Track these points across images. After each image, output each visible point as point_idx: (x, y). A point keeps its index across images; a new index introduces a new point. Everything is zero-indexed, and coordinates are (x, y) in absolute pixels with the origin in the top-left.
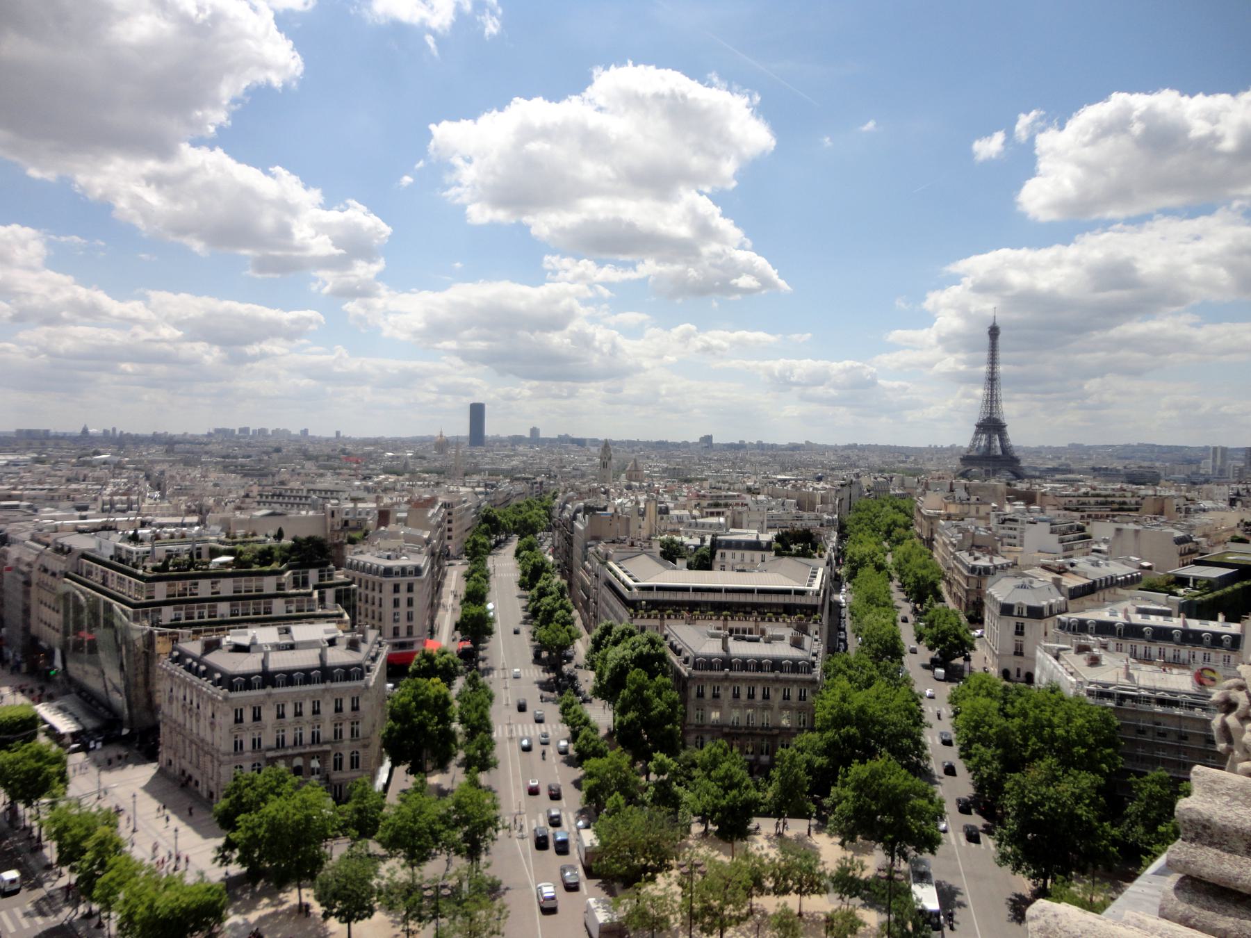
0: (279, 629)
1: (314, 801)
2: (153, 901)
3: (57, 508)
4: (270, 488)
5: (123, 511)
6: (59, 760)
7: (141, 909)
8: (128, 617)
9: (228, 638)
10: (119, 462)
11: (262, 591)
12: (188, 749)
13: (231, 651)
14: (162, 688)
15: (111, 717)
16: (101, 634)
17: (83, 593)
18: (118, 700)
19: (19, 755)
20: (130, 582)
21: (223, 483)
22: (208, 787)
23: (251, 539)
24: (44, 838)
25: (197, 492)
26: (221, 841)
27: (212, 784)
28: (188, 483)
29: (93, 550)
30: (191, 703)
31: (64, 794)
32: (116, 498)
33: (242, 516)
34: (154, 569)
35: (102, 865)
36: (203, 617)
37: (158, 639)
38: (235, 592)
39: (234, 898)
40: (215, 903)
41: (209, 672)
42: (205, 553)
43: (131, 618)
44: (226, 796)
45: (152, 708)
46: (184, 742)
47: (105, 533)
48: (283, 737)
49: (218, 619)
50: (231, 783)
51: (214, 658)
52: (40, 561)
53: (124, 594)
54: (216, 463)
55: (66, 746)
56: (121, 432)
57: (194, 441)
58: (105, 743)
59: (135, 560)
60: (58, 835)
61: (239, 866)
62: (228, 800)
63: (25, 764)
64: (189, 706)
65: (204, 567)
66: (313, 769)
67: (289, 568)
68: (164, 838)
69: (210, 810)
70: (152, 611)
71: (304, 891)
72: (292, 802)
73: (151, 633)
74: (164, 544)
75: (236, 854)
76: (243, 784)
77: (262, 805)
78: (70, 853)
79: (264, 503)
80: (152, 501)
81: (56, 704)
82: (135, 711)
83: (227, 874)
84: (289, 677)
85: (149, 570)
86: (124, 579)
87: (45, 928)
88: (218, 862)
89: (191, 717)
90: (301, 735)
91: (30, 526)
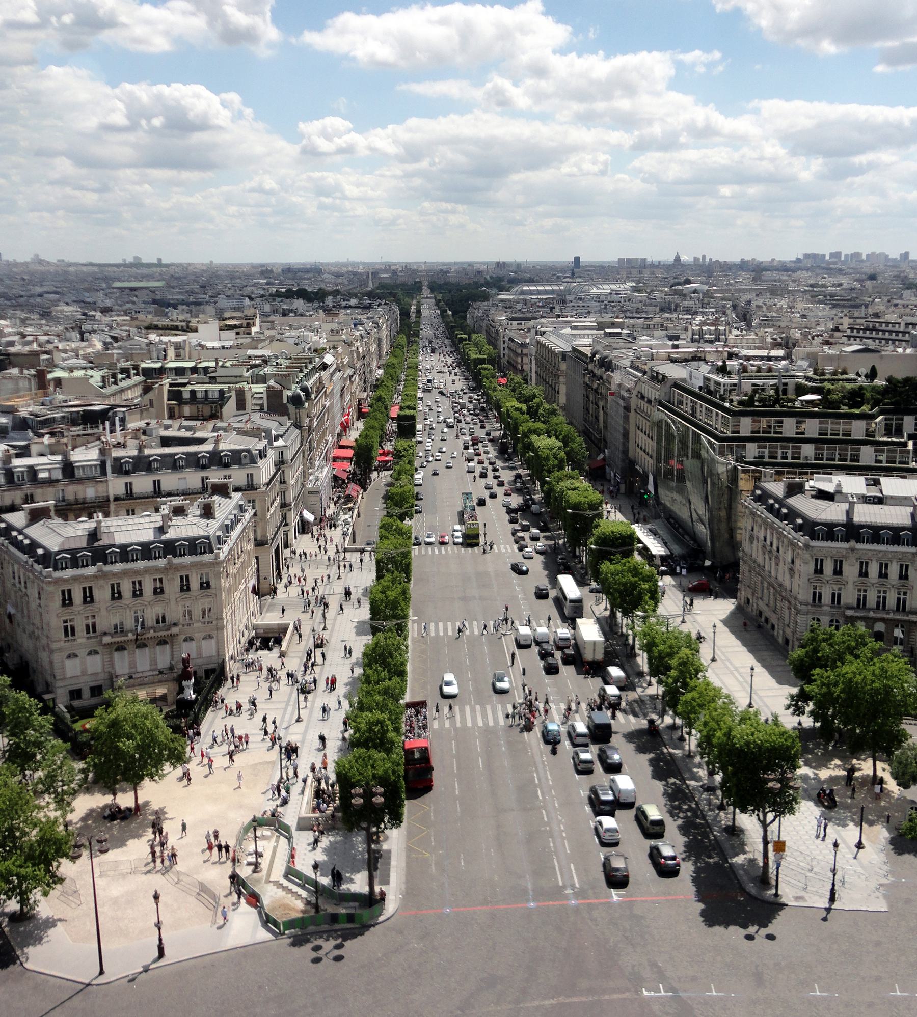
0: (866, 479)
1: (895, 673)
2: (730, 729)
3: (652, 336)
4: (863, 321)
5: (711, 342)
6: (650, 578)
7: (719, 734)
8: (714, 450)
9: (811, 483)
10: (708, 291)
11: (850, 435)
12: (765, 591)
13: (813, 497)
14: (744, 524)
15: (695, 547)
16: (690, 464)
17: (673, 421)
18: (702, 530)
19: (619, 567)
20: (717, 414)
21: (811, 314)
22: (784, 632)
23: (840, 377)
24: (637, 646)
25: (783, 324)
26: (795, 690)
27: (788, 631)
28: (774, 314)
29: (684, 380)
30: (771, 544)
31: (654, 611)
32: (705, 328)
33: (831, 352)
34: (741, 403)
35: (685, 685)
36: (786, 458)
37: (741, 475)
38: (820, 434)
39: (806, 750)
40: (788, 748)
41: (791, 515)
42: (791, 389)
43: (717, 450)
44: (802, 646)
45: (734, 545)
46: (762, 583)
47: (696, 363)
48: (865, 597)
49: (801, 461)
50: (807, 635)
51: (796, 502)
52: (637, 389)
53: (711, 426)
54: (806, 291)
55: (657, 567)
56: (711, 259)
57: (784, 268)
58: (689, 571)
59: (722, 393)
60: (649, 648)
61: (811, 719)
62: (804, 650)
63: (624, 577)
64: (768, 548)
65: (789, 404)
66: (896, 638)
67: (881, 412)
68: (740, 674)
69: (786, 657)
70: (737, 446)
71: (879, 765)
72: (871, 668)
73: (735, 468)
74: (750, 378)
75: (810, 707)
76: (821, 637)
77: (839, 664)
78: (658, 667)
79: (855, 337)
80: (738, 332)
81: (648, 526)
82: (717, 544)
83: (800, 724)
84: (876, 533)
85: (735, 403)
86: (712, 412)
87: (638, 727)
88: (791, 710)
89: (770, 559)
90: (885, 598)
91: (630, 353)
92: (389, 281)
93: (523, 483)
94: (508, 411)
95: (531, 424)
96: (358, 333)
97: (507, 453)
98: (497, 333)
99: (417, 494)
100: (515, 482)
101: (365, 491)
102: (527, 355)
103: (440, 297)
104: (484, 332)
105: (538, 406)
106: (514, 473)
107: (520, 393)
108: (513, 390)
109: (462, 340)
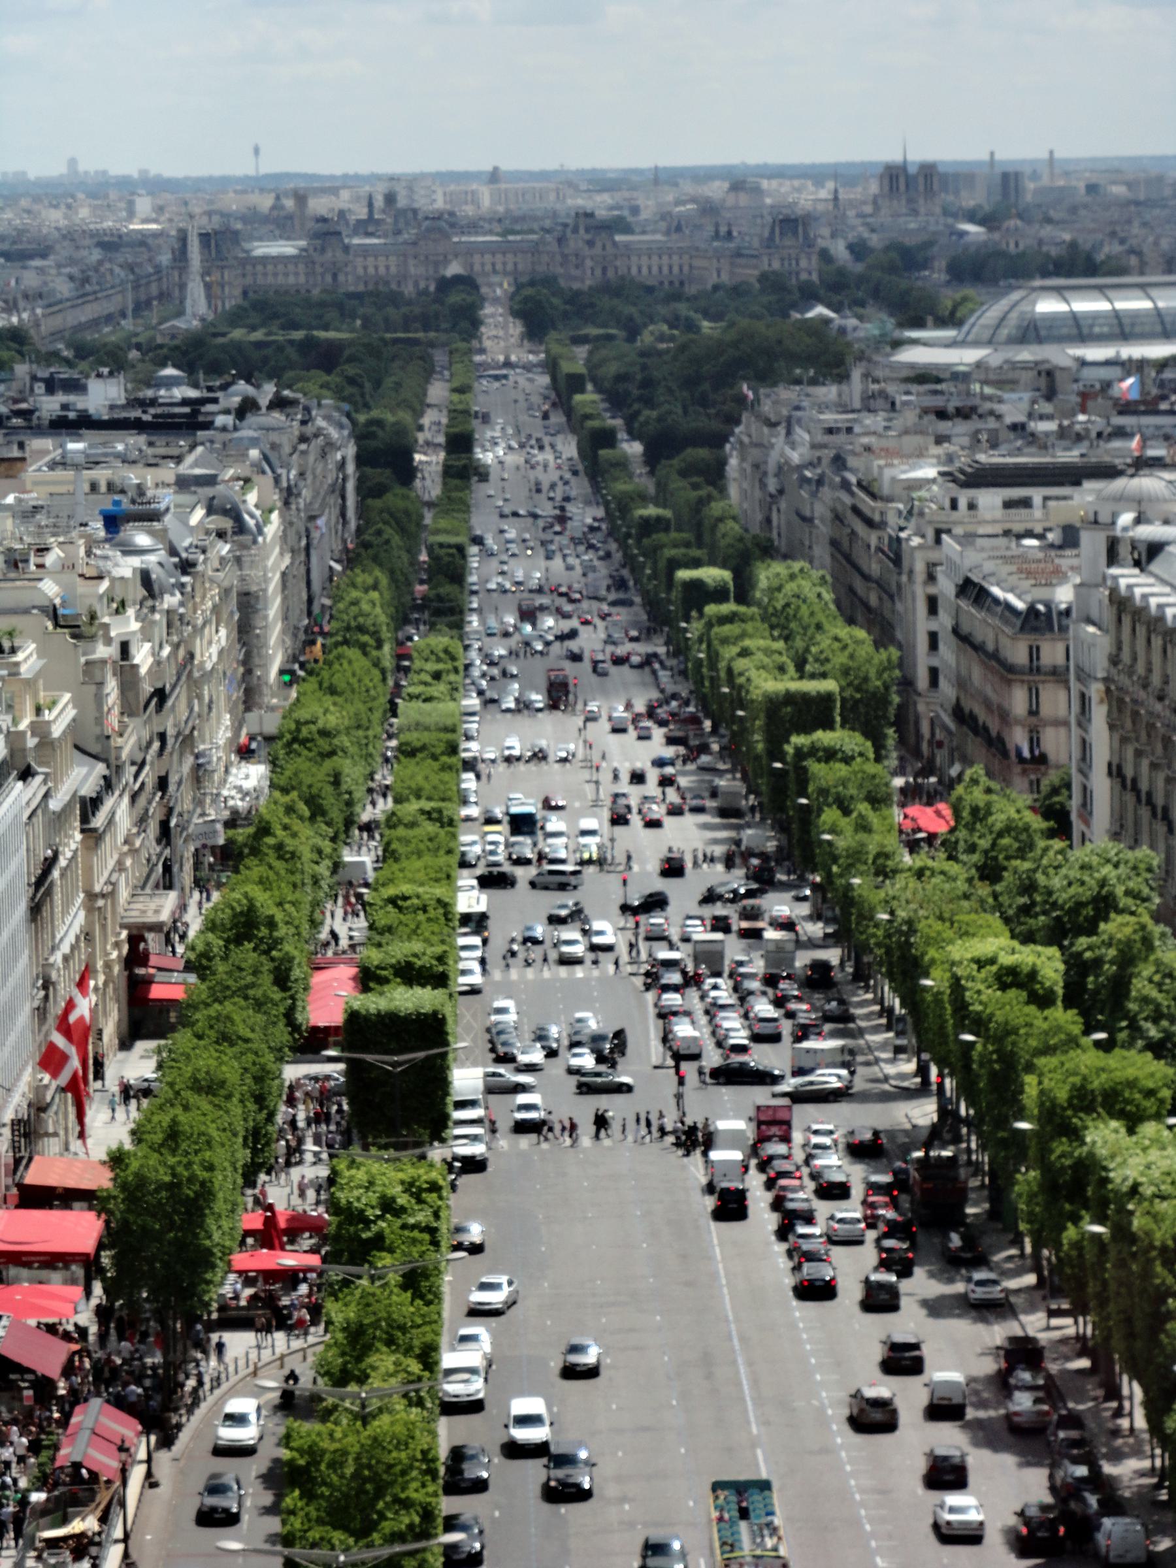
92: (295, 279)
93: (1051, 1391)
94: (957, 985)
95: (1086, 1059)
96: (126, 567)
97: (956, 1220)
98: (895, 554)
99: (458, 1455)
100: (1003, 1383)
101: (167, 1442)
102: (1058, 675)
103: (577, 360)
104: (822, 551)
105: (1128, 959)
106: (998, 1333)
107: (1028, 887)
108: (990, 872)
109: (698, 594)
